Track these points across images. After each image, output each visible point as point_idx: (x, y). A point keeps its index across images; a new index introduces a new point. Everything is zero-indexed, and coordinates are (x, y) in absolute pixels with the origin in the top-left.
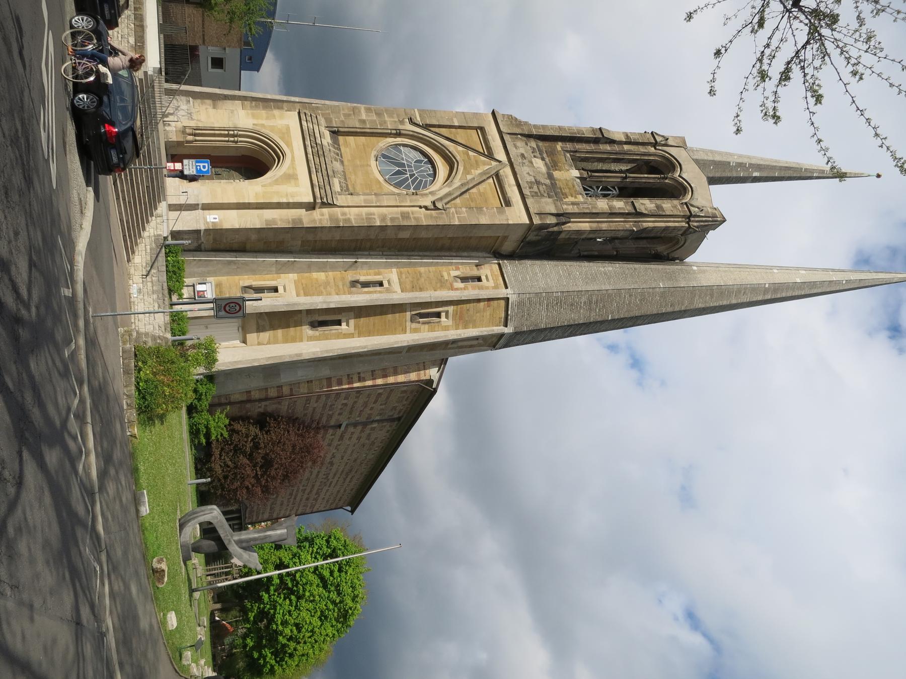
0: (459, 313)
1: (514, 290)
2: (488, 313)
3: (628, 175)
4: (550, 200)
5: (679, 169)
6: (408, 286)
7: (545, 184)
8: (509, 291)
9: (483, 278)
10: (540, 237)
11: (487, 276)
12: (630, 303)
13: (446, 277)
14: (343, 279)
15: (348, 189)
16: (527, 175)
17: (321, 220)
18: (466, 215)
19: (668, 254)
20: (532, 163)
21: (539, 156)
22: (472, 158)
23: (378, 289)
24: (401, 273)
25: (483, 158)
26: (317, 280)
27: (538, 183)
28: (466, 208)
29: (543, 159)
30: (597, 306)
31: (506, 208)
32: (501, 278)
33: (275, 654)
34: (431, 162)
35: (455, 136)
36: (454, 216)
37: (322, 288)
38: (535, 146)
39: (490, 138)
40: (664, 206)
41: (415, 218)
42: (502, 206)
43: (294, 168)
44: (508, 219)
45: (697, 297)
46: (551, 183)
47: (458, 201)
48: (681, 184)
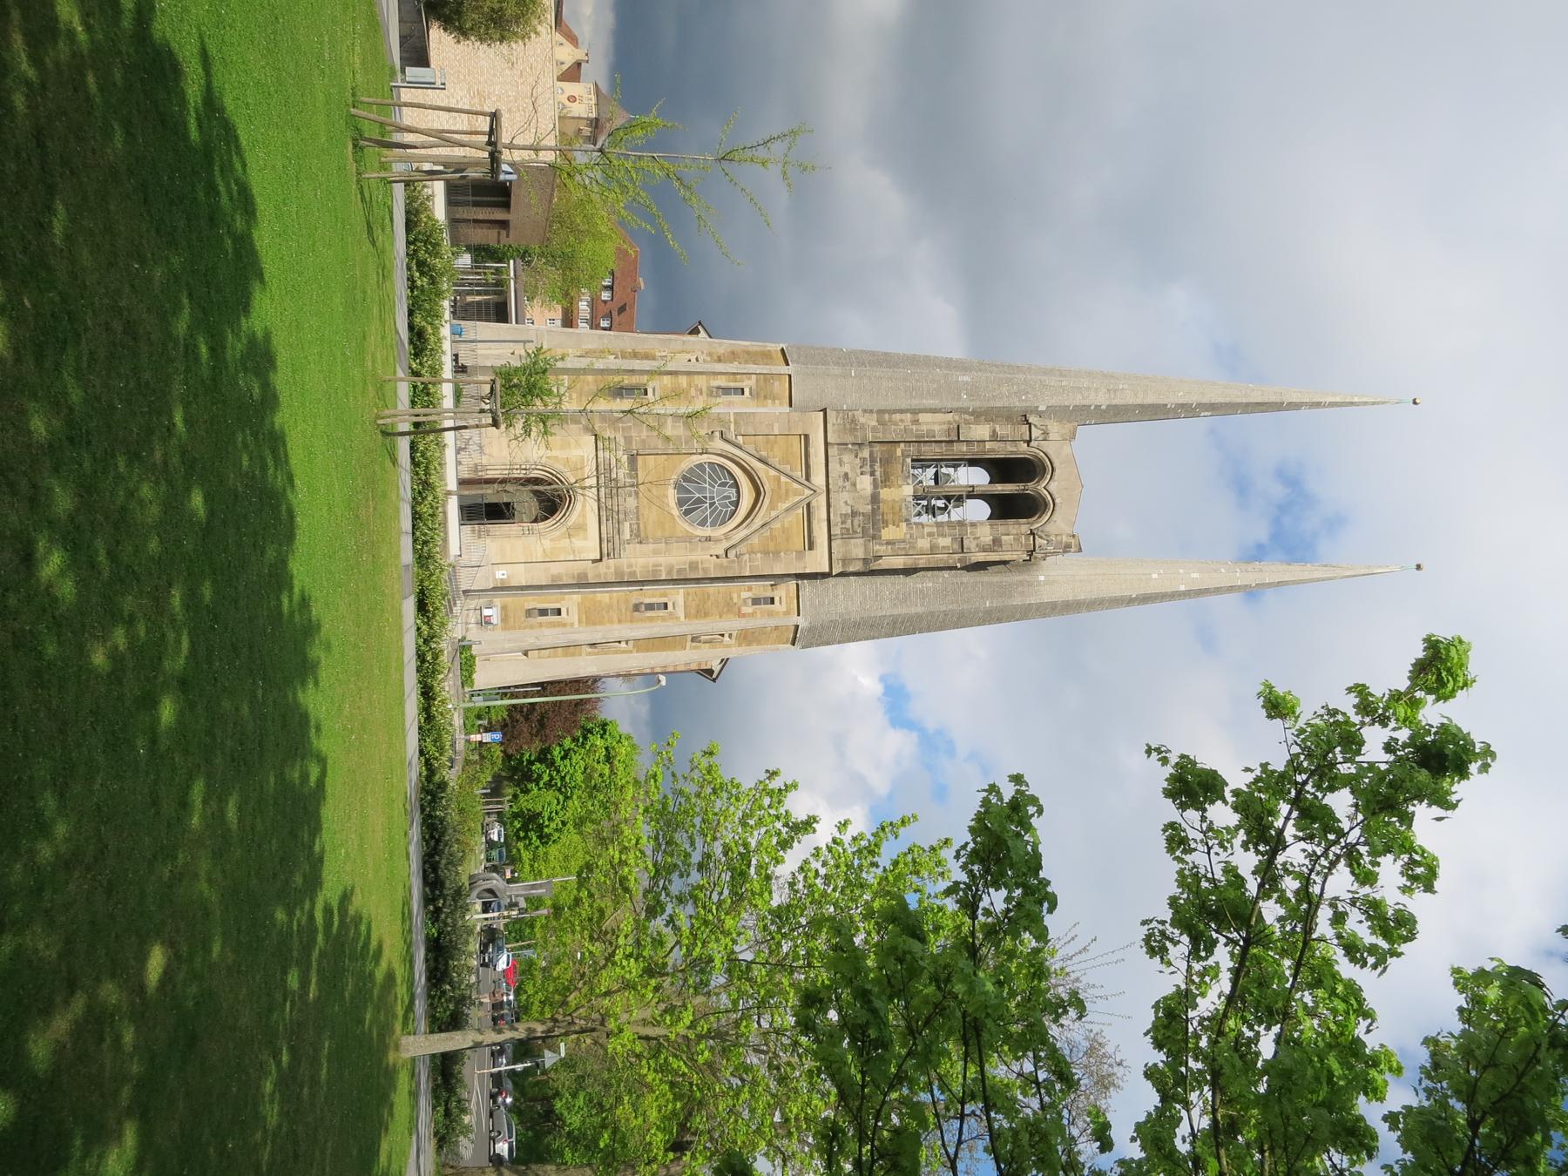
5: (1049, 476)
6: (693, 612)
9: (777, 600)
13: (735, 601)
14: (627, 601)
15: (638, 536)
16: (842, 504)
17: (606, 574)
23: (662, 613)
24: (688, 594)
25: (796, 485)
26: (600, 602)
31: (807, 552)
32: (795, 601)
33: (540, 837)
34: (736, 485)
37: (604, 613)
39: (812, 450)
41: (703, 569)
43: (584, 516)
48: (1044, 500)
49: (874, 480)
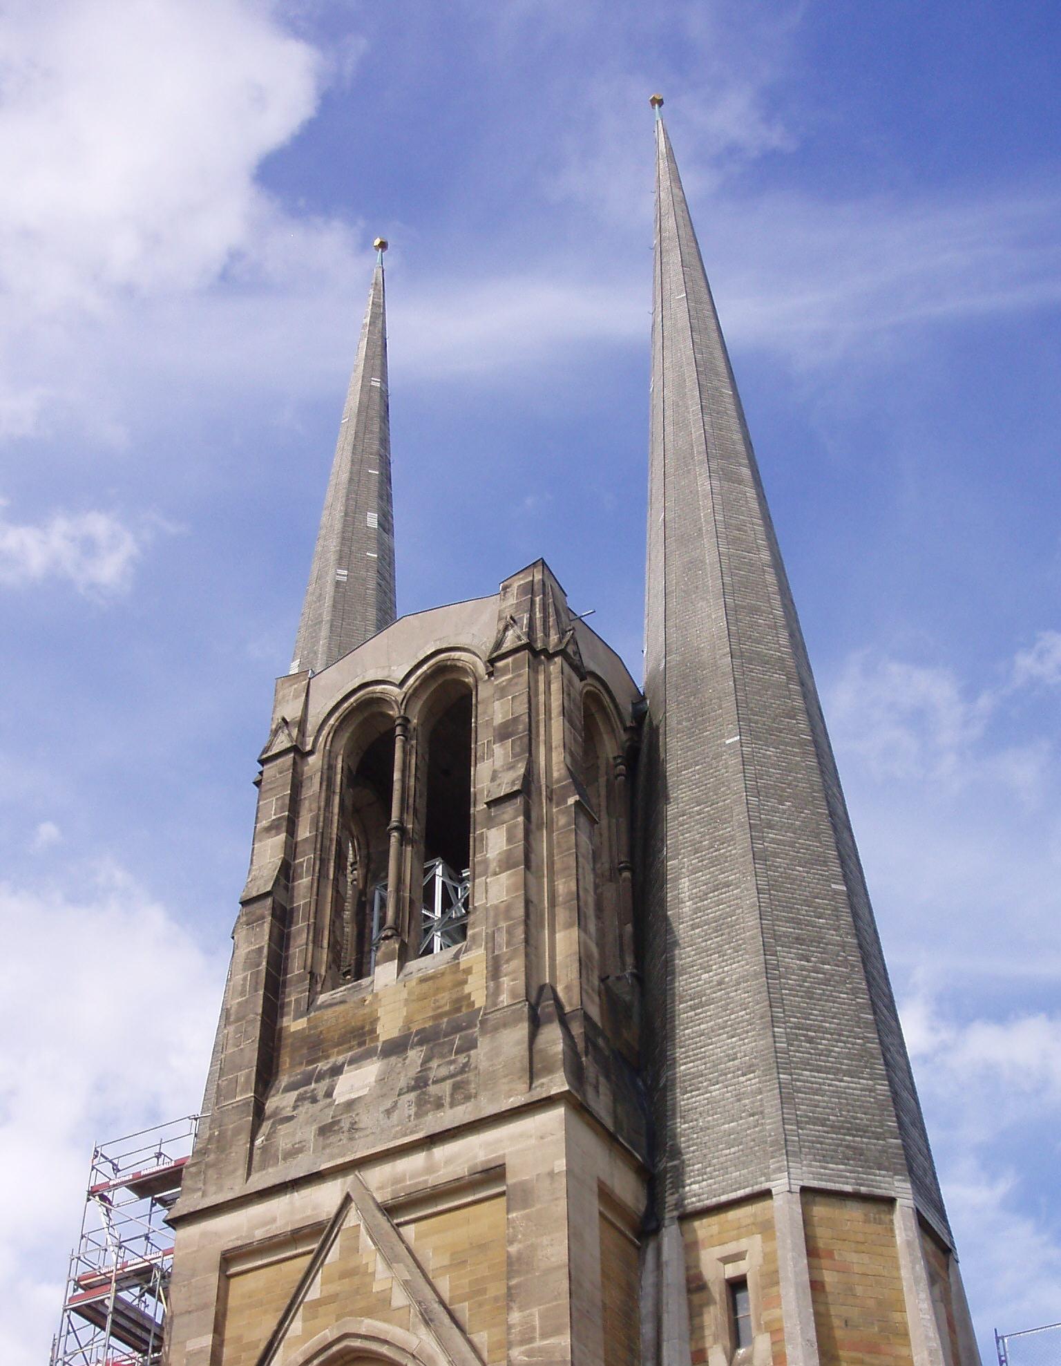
0: (860, 1355)
1: (779, 1170)
2: (854, 1257)
3: (395, 824)
4: (484, 1045)
5: (379, 688)
7: (425, 1062)
8: (779, 1185)
9: (731, 1271)
10: (602, 1079)
11: (726, 1260)
12: (790, 828)
16: (395, 1116)
18: (535, 1311)
19: (626, 729)
20: (350, 1105)
21: (327, 1081)
22: (334, 1288)
25: (333, 1255)
27: (420, 1083)
28: (509, 1309)
29: (336, 1071)
30: (809, 924)
31: (511, 1180)
32: (732, 1215)
35: (252, 1346)
36: (541, 1350)
38: (293, 1095)
39: (259, 1234)
40: (499, 719)
42: (503, 1194)
44: (551, 1175)
45: (761, 648)
46: (420, 1043)
47: (482, 1338)
49: (352, 1062)
